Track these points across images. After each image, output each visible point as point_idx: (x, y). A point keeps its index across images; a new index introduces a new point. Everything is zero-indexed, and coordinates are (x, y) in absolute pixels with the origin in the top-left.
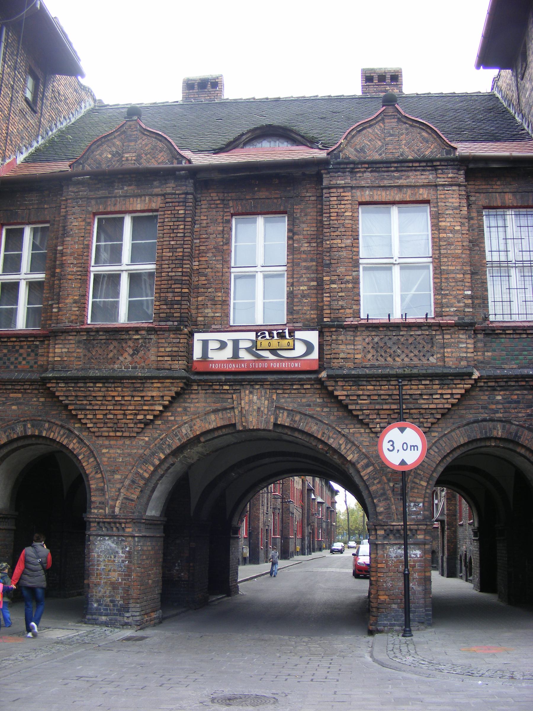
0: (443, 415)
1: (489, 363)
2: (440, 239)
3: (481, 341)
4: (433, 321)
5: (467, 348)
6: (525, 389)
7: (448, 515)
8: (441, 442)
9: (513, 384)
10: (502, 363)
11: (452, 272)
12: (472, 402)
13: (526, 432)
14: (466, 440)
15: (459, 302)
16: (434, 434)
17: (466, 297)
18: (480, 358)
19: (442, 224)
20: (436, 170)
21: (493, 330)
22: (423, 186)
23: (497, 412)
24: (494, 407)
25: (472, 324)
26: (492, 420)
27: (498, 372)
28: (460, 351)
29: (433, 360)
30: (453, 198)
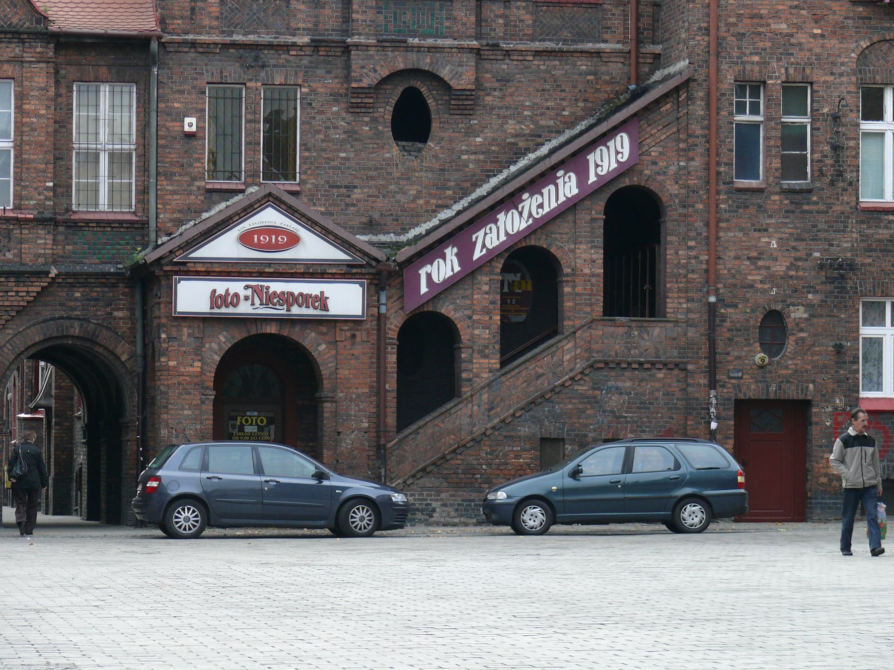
0: (17, 312)
1: (69, 257)
2: (23, 125)
3: (62, 233)
4: (11, 215)
5: (46, 244)
6: (106, 286)
7: (57, 398)
8: (15, 339)
9: (93, 281)
10: (84, 258)
11: (33, 161)
12: (49, 299)
13: (105, 331)
14: (42, 338)
15: (39, 194)
16: (8, 331)
17: (47, 189)
18: (60, 252)
19: (26, 107)
20: (23, 43)
21: (75, 222)
22: (8, 61)
23: (75, 309)
24: (72, 304)
25: (51, 219)
27: (78, 268)
28: (38, 247)
29: (9, 255)
30: (40, 78)
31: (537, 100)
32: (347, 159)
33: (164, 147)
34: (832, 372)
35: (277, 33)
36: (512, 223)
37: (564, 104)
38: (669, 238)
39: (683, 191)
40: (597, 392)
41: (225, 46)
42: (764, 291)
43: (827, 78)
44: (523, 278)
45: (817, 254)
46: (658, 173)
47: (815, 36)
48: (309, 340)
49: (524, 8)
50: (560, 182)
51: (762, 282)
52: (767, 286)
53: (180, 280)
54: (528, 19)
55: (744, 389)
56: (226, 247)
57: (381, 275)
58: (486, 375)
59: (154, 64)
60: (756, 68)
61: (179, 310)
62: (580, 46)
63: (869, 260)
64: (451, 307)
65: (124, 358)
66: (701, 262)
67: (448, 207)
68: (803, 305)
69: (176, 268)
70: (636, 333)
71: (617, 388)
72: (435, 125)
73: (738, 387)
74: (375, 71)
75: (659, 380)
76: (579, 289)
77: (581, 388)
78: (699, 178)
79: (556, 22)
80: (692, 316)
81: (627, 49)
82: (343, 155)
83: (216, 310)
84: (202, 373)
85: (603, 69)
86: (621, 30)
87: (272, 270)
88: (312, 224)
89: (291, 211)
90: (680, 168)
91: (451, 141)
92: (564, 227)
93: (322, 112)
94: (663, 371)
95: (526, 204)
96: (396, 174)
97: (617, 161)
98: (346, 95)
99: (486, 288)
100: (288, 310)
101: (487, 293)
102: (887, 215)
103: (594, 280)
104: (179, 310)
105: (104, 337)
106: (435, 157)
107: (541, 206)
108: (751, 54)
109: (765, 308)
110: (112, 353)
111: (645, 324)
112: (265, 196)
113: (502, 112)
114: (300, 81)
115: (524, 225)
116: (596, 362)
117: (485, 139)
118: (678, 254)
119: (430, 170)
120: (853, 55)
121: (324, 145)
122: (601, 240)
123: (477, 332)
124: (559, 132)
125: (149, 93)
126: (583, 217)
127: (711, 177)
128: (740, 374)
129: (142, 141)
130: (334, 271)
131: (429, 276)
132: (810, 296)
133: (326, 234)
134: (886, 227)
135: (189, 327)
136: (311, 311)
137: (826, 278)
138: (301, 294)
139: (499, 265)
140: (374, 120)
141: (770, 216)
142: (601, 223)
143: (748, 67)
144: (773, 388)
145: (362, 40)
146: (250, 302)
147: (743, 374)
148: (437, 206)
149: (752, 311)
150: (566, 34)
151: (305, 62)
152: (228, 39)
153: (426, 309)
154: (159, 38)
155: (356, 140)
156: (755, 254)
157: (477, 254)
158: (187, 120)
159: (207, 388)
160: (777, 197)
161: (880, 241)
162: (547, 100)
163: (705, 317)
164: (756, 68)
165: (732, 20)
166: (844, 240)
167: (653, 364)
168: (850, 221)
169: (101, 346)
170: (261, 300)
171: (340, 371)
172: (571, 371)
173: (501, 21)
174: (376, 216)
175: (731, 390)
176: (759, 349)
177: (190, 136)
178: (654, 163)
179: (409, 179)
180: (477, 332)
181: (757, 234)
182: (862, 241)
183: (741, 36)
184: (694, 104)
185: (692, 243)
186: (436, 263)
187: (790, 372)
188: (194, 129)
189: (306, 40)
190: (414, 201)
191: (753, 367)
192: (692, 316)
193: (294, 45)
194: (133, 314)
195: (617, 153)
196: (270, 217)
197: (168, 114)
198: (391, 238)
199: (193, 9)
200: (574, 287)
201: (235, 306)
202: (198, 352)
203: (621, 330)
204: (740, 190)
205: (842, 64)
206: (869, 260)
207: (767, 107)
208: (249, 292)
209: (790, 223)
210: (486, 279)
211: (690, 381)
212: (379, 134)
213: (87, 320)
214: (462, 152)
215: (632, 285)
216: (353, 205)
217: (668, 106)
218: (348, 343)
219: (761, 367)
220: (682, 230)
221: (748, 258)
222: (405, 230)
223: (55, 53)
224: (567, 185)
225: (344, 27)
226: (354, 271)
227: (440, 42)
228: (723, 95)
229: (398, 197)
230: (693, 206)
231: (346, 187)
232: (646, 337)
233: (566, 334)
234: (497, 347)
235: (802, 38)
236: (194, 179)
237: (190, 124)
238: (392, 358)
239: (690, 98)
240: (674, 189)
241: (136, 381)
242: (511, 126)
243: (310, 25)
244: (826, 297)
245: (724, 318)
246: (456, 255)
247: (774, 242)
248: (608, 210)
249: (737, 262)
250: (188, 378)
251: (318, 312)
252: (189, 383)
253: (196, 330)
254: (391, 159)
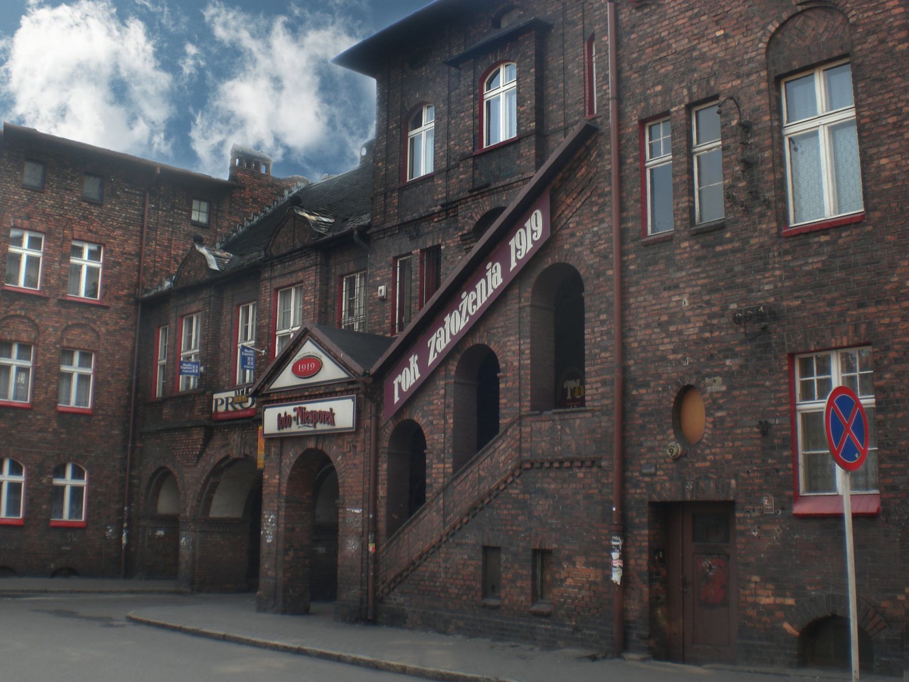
34: (758, 461)
36: (455, 323)
39: (597, 260)
40: (528, 496)
42: (679, 362)
43: (735, 83)
45: (733, 306)
46: (576, 246)
47: (717, 40)
51: (674, 351)
52: (680, 356)
63: (797, 303)
68: (720, 375)
70: (559, 427)
73: (651, 486)
83: (282, 431)
94: (583, 470)
95: (464, 302)
100: (315, 427)
102: (818, 236)
107: (475, 303)
108: (653, 86)
109: (677, 384)
111: (566, 416)
115: (463, 324)
120: (761, 45)
126: (512, 307)
128: (653, 470)
132: (728, 362)
134: (818, 254)
137: (746, 334)
141: (681, 269)
144: (690, 486)
147: (656, 469)
149: (665, 389)
156: (664, 318)
161: (810, 273)
166: (766, 281)
168: (771, 254)
175: (644, 491)
176: (673, 436)
178: (573, 235)
181: (665, 294)
182: (788, 278)
185: (603, 317)
187: (708, 464)
191: (668, 460)
203: (546, 425)
205: (751, 60)
206: (797, 303)
209: (702, 272)
217: (584, 169)
219: (676, 459)
221: (659, 325)
224: (494, 276)
230: (605, 274)
232: (568, 431)
235: (704, 47)
240: (591, 259)
244: (747, 360)
247: (685, 299)
249: (648, 331)
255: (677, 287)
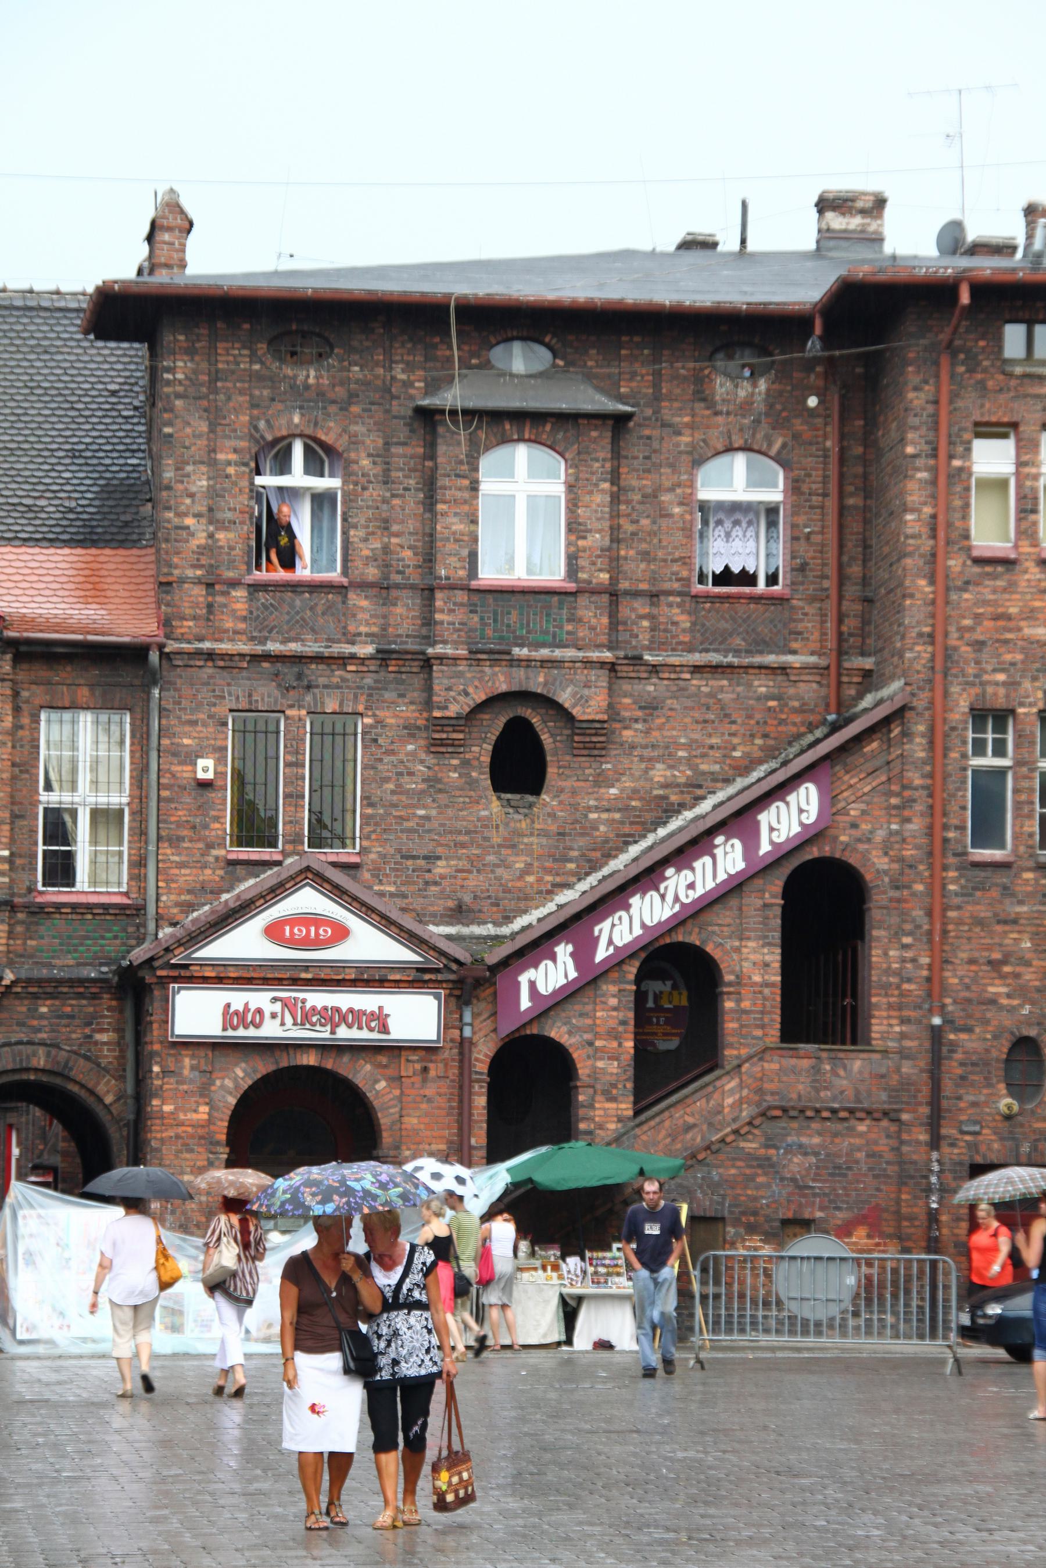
1: (31, 956)
13: (82, 1062)
18: (20, 950)
21: (41, 907)
23: (39, 1030)
24: (35, 1023)
26: (30, 1043)
31: (696, 736)
32: (427, 818)
33: (169, 800)
35: (329, 640)
37: (735, 740)
38: (875, 933)
40: (772, 1152)
41: (256, 658)
42: (1012, 1010)
44: (675, 987)
46: (859, 840)
48: (363, 1074)
49: (679, 605)
50: (719, 852)
51: (1009, 996)
53: (180, 989)
54: (685, 621)
55: (983, 1148)
56: (245, 942)
57: (467, 983)
58: (612, 1126)
59: (155, 683)
60: (1002, 691)
61: (177, 1032)
62: (757, 660)
64: (565, 1029)
65: (109, 1099)
66: (921, 967)
67: (568, 886)
69: (174, 973)
70: (828, 1067)
71: (801, 1146)
72: (551, 771)
73: (973, 1147)
74: (467, 694)
75: (861, 1135)
76: (746, 1004)
77: (750, 1146)
78: (917, 847)
79: (724, 625)
80: (907, 1043)
81: (823, 662)
82: (421, 812)
83: (230, 1033)
84: (210, 1121)
85: (791, 691)
86: (816, 636)
87: (309, 976)
88: (367, 911)
89: (338, 893)
90: (891, 833)
91: (574, 792)
92: (724, 917)
93: (392, 752)
94: (868, 1122)
96: (496, 840)
97: (801, 824)
98: (427, 728)
99: (613, 1002)
100: (333, 1032)
101: (615, 1009)
103: (767, 991)
104: (177, 1032)
105: (80, 1070)
106: (552, 815)
107: (691, 886)
108: (995, 670)
109: (1012, 1033)
110: (92, 1092)
111: (841, 1055)
112: (301, 872)
113: (647, 753)
114: (361, 708)
115: (667, 913)
116: (770, 1108)
117: (622, 790)
118: (890, 955)
119: (544, 833)
121: (395, 798)
122: (778, 935)
123: (600, 1064)
124: (728, 781)
125: (148, 725)
126: (752, 901)
127: (936, 847)
128: (977, 1128)
129: (137, 793)
130: (398, 977)
131: (532, 984)
133: (386, 923)
135: (193, 1057)
136: (364, 1034)
138: (351, 1010)
139: (632, 970)
140: (466, 763)
141: (1021, 903)
142: (778, 911)
143: (990, 690)
145: (449, 650)
146: (278, 1020)
148: (555, 885)
149: (995, 1037)
150: (738, 642)
151: (369, 681)
152: (259, 649)
153: (528, 1032)
154: (161, 647)
155: (440, 791)
156: (997, 956)
157: (602, 953)
158: (201, 763)
159: (218, 1143)
160: (1029, 875)
162: (710, 735)
163: (927, 1045)
164: (1002, 691)
165: (967, 622)
167: (852, 1111)
169: (76, 1082)
170: (294, 1018)
171: (406, 1119)
172: (734, 1120)
173: (646, 623)
174: (467, 898)
176: (1004, 1092)
177: (205, 785)
178: (854, 826)
179: (514, 846)
180: (600, 1064)
181: (999, 928)
183: (979, 645)
184: (911, 741)
185: (907, 940)
186: (542, 966)
188: (210, 775)
189: (369, 650)
190: (521, 878)
192: (907, 1043)
193: (353, 657)
194: (122, 1037)
195: (801, 811)
196: (308, 900)
197: (174, 755)
198: (489, 929)
199: (210, 606)
200: (738, 1001)
201: (257, 1026)
202: (204, 1091)
203: (805, 1063)
204: (976, 865)
207: (1017, 746)
208: (277, 1007)
210: (613, 989)
211: (905, 1137)
212: (472, 784)
213: (57, 1046)
214: (589, 809)
215: (822, 998)
216: (436, 883)
217: (875, 745)
218: (417, 1079)
219: (1008, 1118)
220: (894, 920)
222: (508, 919)
223: (14, 667)
225: (424, 631)
226: (427, 977)
227: (558, 653)
228: (953, 729)
229: (499, 871)
230: (909, 887)
231: (425, 858)
232: (842, 1073)
233: (728, 1067)
234: (630, 1085)
236: (210, 846)
237: (205, 768)
238: (481, 1101)
239: (906, 734)
240: (881, 862)
241: (125, 1133)
242: (660, 773)
243: (375, 629)
245: (953, 1046)
246: (572, 955)
248: (789, 892)
250: (189, 1129)
251: (375, 1035)
252: (192, 1136)
253: (203, 1061)
254: (489, 818)
255: (1015, 922)
